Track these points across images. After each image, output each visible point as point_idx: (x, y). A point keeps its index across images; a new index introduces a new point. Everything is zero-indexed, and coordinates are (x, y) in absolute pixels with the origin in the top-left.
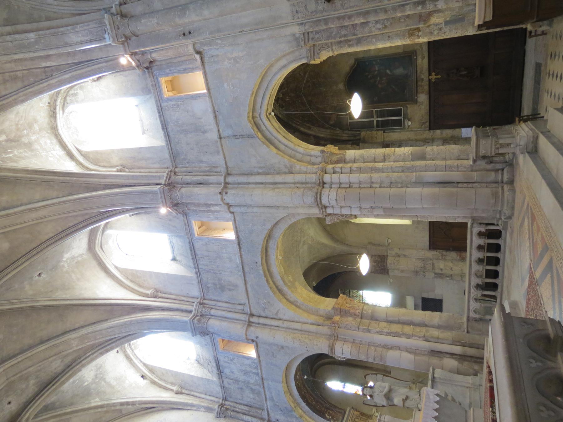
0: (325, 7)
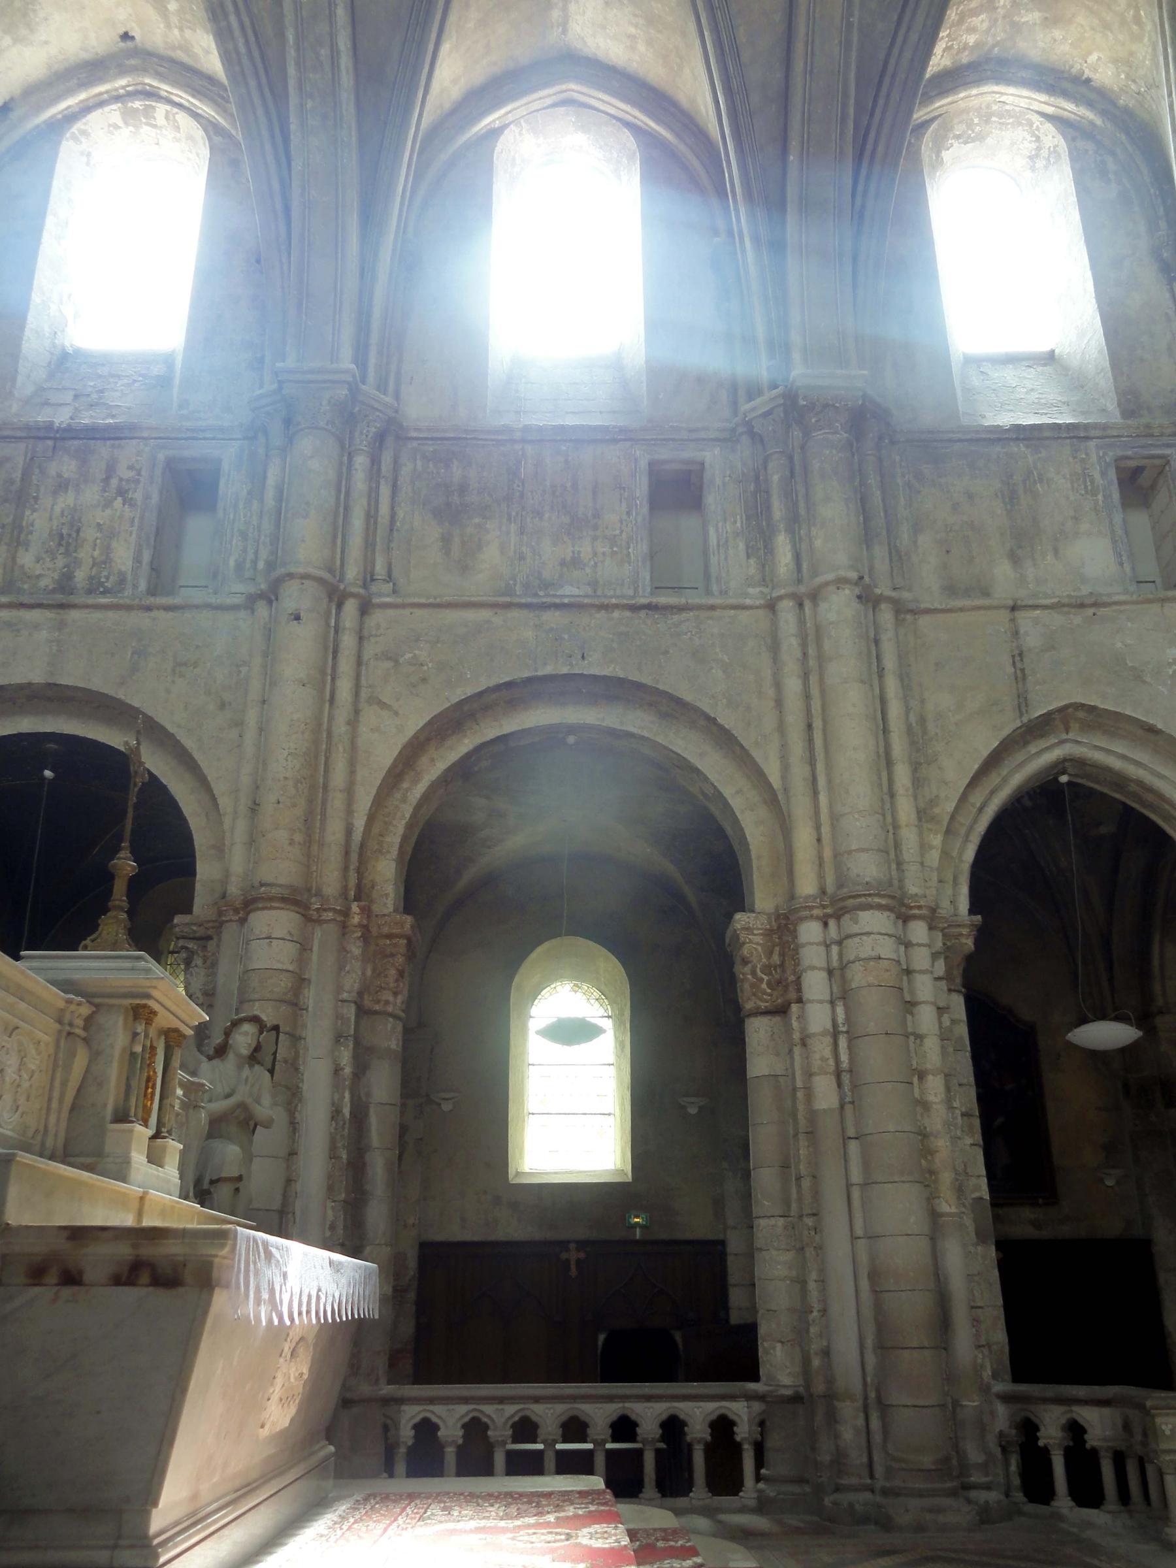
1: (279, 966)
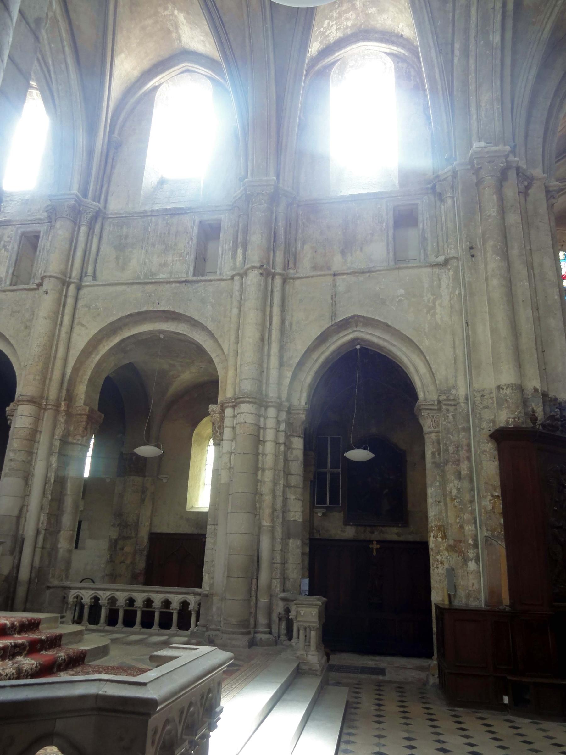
0: (484, 431)
1: (24, 426)
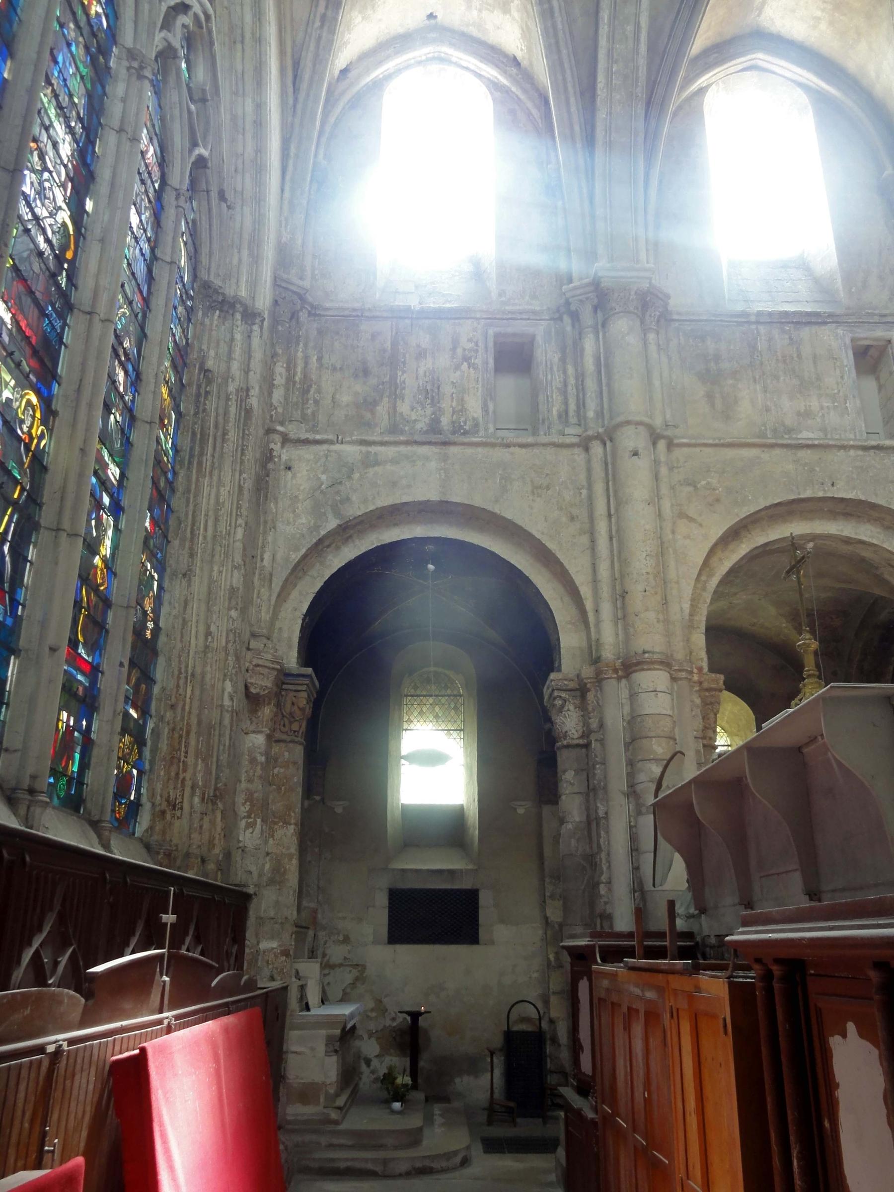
1: (664, 712)
